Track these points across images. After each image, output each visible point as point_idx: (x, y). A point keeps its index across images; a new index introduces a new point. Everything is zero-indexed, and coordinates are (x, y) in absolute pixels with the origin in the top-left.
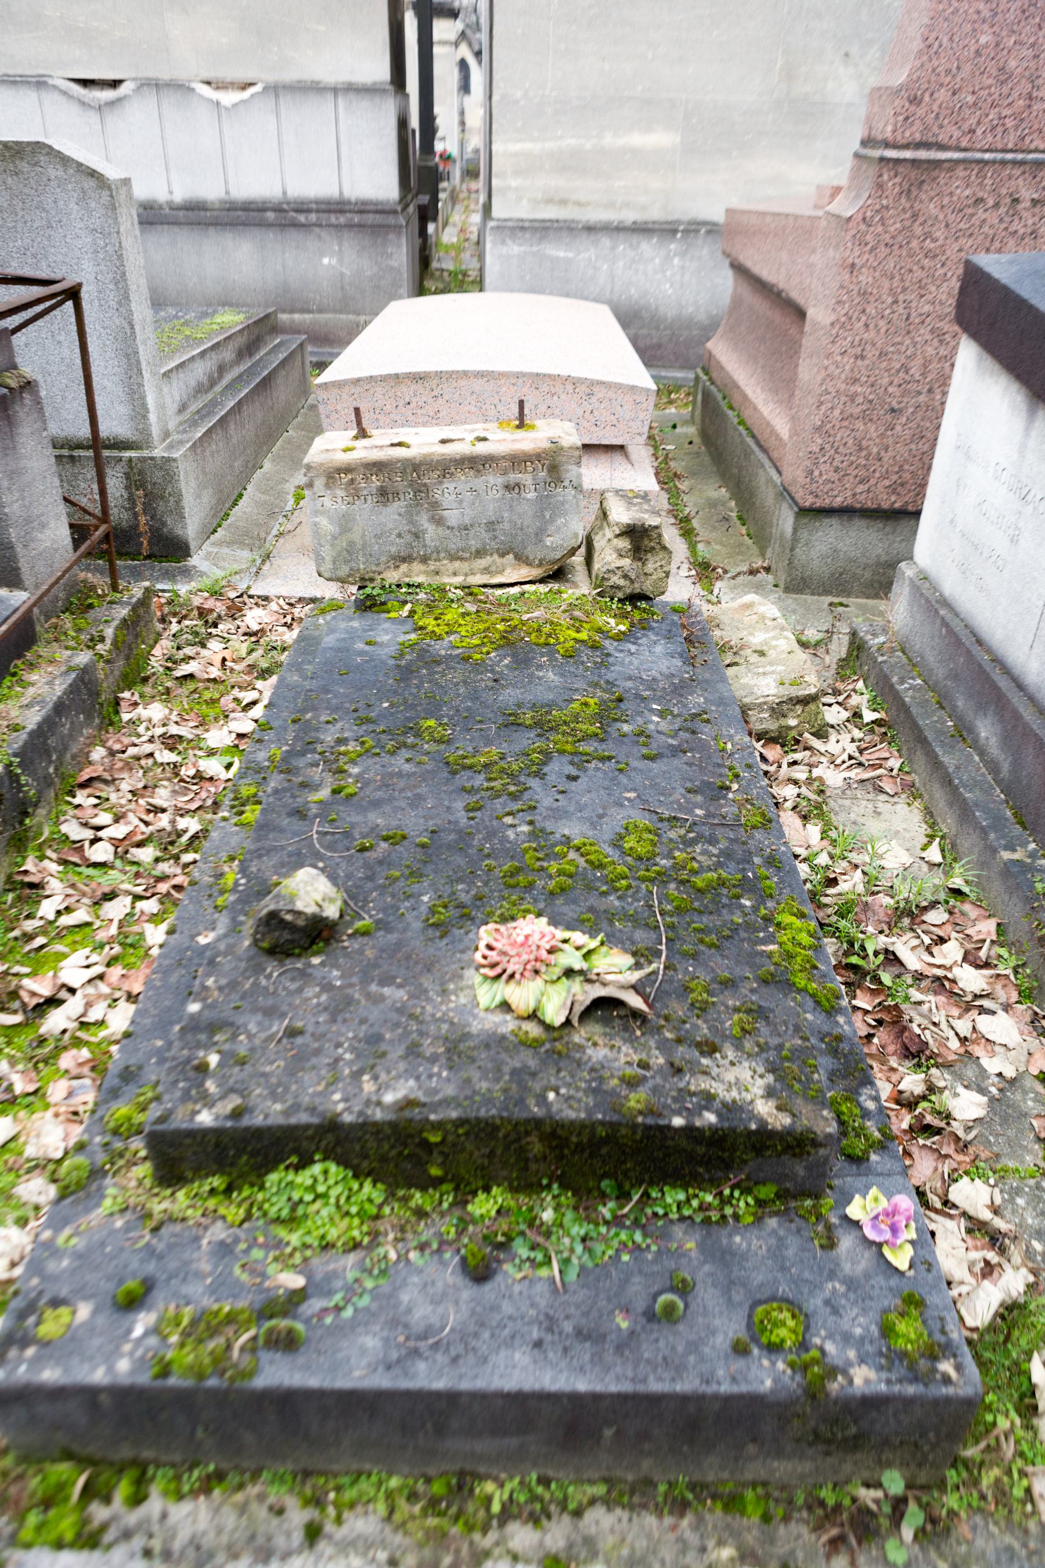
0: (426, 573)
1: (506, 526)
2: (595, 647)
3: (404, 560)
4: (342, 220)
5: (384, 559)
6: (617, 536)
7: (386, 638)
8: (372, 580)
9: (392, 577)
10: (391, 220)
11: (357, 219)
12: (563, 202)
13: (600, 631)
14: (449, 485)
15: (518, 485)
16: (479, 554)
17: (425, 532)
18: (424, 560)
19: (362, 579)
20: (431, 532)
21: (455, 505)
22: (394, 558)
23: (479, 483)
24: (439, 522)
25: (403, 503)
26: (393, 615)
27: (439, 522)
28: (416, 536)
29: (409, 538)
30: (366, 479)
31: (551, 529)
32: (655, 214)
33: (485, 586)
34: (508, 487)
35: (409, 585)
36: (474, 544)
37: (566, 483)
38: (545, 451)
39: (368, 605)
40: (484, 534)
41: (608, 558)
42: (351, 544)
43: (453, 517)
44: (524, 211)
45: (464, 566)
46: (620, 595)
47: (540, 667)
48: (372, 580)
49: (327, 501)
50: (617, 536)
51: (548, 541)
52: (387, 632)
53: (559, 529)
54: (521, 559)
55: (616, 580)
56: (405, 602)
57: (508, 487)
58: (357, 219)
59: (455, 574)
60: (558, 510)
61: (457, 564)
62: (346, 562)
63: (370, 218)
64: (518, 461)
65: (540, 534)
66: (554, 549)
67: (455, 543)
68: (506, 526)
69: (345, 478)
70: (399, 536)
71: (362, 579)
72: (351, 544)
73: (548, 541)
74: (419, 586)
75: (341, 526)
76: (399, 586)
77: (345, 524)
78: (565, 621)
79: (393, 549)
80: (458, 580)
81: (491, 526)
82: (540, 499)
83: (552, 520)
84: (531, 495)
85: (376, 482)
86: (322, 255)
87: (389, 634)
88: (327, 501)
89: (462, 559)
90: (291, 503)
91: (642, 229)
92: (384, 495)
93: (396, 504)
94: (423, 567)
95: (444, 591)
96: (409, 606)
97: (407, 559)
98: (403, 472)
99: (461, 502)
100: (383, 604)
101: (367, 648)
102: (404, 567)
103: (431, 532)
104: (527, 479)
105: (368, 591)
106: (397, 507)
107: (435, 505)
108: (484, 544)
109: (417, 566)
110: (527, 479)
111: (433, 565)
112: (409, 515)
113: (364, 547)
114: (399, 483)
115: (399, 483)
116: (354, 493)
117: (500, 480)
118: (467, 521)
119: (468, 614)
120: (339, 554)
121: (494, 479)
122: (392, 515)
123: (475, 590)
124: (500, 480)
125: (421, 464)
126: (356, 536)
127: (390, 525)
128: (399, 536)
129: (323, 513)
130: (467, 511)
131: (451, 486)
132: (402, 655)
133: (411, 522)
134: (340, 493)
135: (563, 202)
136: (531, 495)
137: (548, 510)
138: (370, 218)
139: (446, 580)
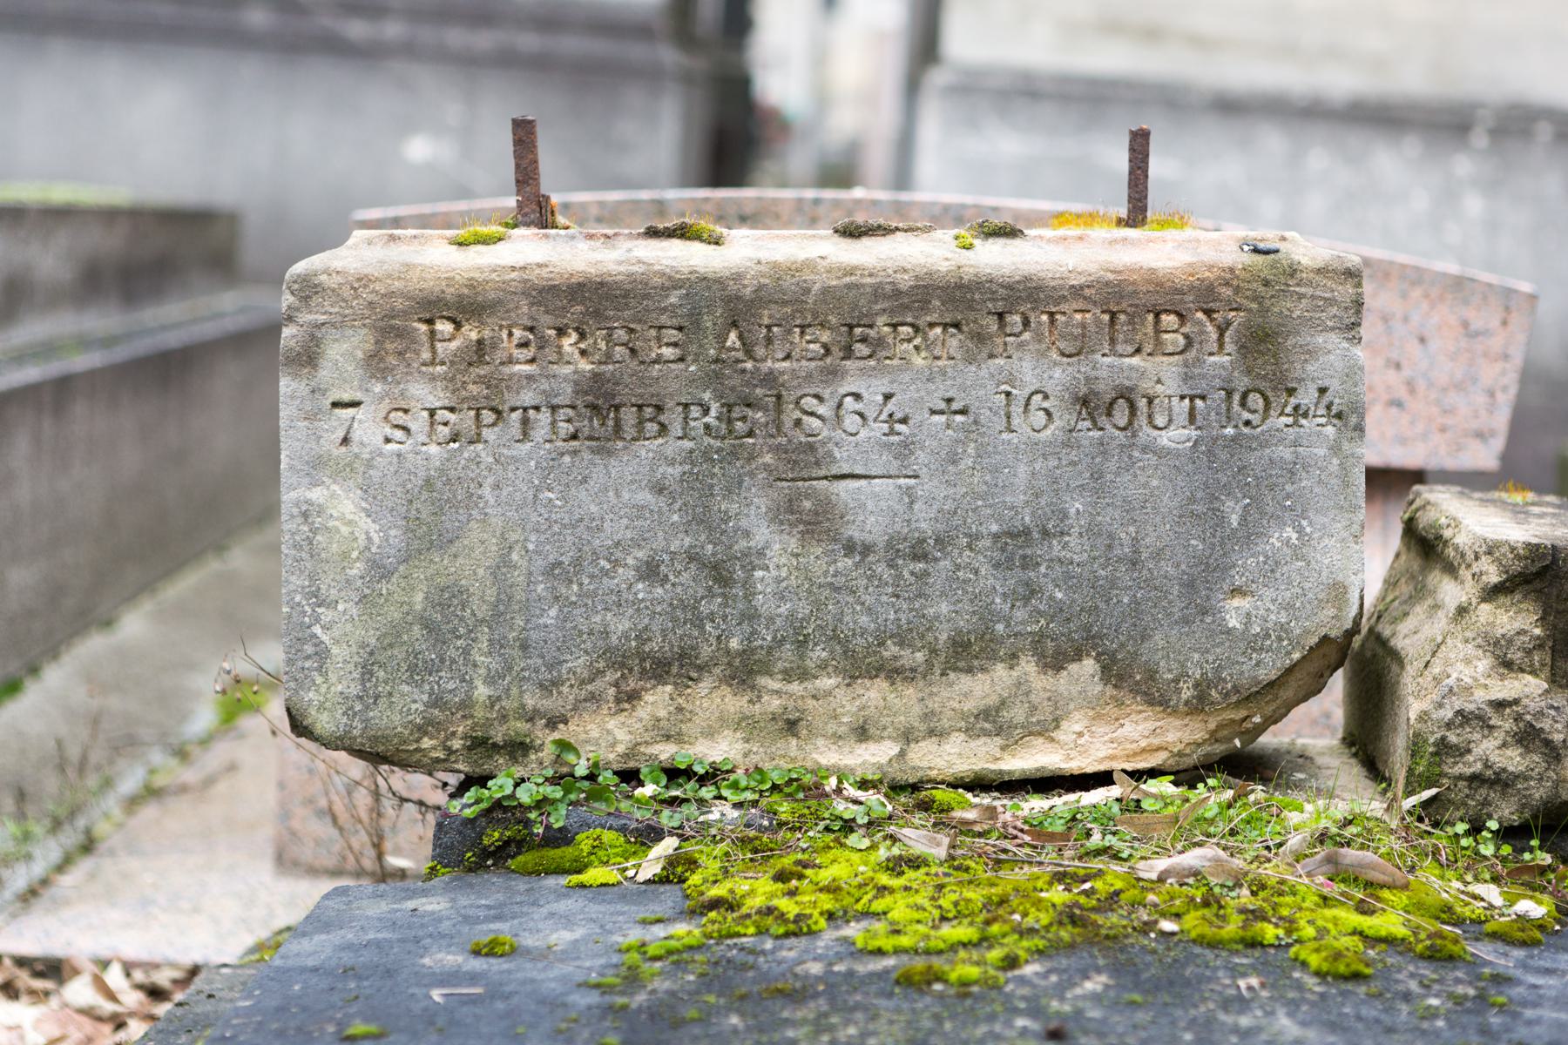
0: (747, 725)
1: (1076, 547)
2: (1438, 955)
3: (659, 669)
4: (484, 40)
5: (578, 663)
6: (1492, 593)
7: (562, 937)
8: (518, 749)
9: (604, 736)
10: (636, 52)
11: (528, 41)
12: (1152, 34)
13: (1446, 913)
14: (864, 384)
15: (1126, 395)
16: (966, 653)
17: (753, 559)
18: (744, 672)
19: (480, 744)
20: (777, 557)
21: (881, 462)
22: (618, 659)
23: (979, 382)
24: (815, 523)
25: (673, 446)
26: (595, 875)
27: (815, 523)
28: (719, 574)
29: (687, 581)
30: (538, 343)
31: (1247, 564)
32: (1411, 79)
33: (978, 784)
34: (1088, 404)
35: (674, 774)
36: (946, 613)
37: (1306, 397)
38: (1230, 278)
39: (493, 845)
40: (988, 578)
41: (1461, 673)
42: (449, 598)
43: (871, 506)
44: (1037, 50)
45: (905, 702)
46: (1505, 811)
47: (1241, 1003)
48: (518, 749)
49: (368, 427)
50: (1492, 593)
51: (1234, 611)
52: (568, 921)
53: (1272, 567)
54: (1130, 679)
55: (1493, 750)
56: (652, 834)
57: (1088, 404)
58: (528, 41)
59: (862, 733)
60: (1273, 494)
61: (875, 693)
62: (417, 670)
63: (571, 45)
64: (1128, 308)
65: (1205, 581)
66: (1254, 644)
67: (870, 610)
68: (1076, 547)
69: (453, 340)
70: (650, 571)
71: (480, 744)
72: (449, 598)
73: (1234, 611)
74: (712, 776)
75: (412, 524)
76: (630, 777)
77: (431, 515)
78: (1309, 883)
79: (620, 625)
80: (875, 755)
81: (1018, 545)
82: (1207, 450)
83: (1249, 534)
84: (1176, 436)
85: (574, 359)
86: (408, 127)
87: (571, 931)
88: (368, 427)
89: (895, 673)
90: (204, 718)
91: (1379, 117)
92: (603, 411)
93: (646, 449)
94: (734, 703)
95: (815, 791)
96: (668, 845)
97: (673, 667)
98: (689, 326)
99: (905, 449)
100: (560, 838)
101: (478, 964)
102: (657, 700)
103: (777, 557)
104: (1161, 374)
105: (501, 786)
106: (646, 460)
107: (804, 459)
108: (987, 616)
109: (711, 698)
110: (1161, 374)
111: (775, 695)
112: (697, 494)
113: (498, 616)
114: (669, 367)
115: (669, 367)
116: (484, 399)
117: (1059, 376)
118: (925, 522)
119: (915, 863)
120: (393, 636)
121: (1038, 370)
122: (626, 491)
123: (942, 795)
124: (1059, 376)
125: (762, 298)
126: (471, 564)
127: (615, 529)
128: (650, 571)
129: (343, 471)
130: (928, 486)
131: (873, 391)
132: (632, 979)
133: (701, 519)
134: (424, 393)
135: (1152, 34)
136: (1176, 436)
137: (1235, 491)
138: (571, 45)
139: (827, 755)
